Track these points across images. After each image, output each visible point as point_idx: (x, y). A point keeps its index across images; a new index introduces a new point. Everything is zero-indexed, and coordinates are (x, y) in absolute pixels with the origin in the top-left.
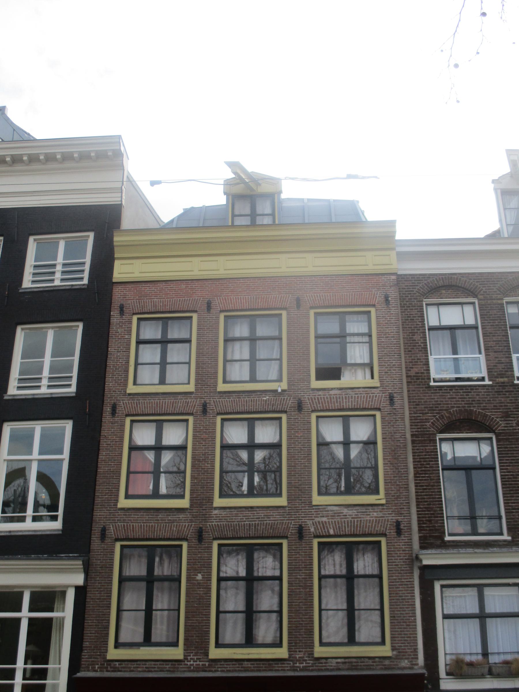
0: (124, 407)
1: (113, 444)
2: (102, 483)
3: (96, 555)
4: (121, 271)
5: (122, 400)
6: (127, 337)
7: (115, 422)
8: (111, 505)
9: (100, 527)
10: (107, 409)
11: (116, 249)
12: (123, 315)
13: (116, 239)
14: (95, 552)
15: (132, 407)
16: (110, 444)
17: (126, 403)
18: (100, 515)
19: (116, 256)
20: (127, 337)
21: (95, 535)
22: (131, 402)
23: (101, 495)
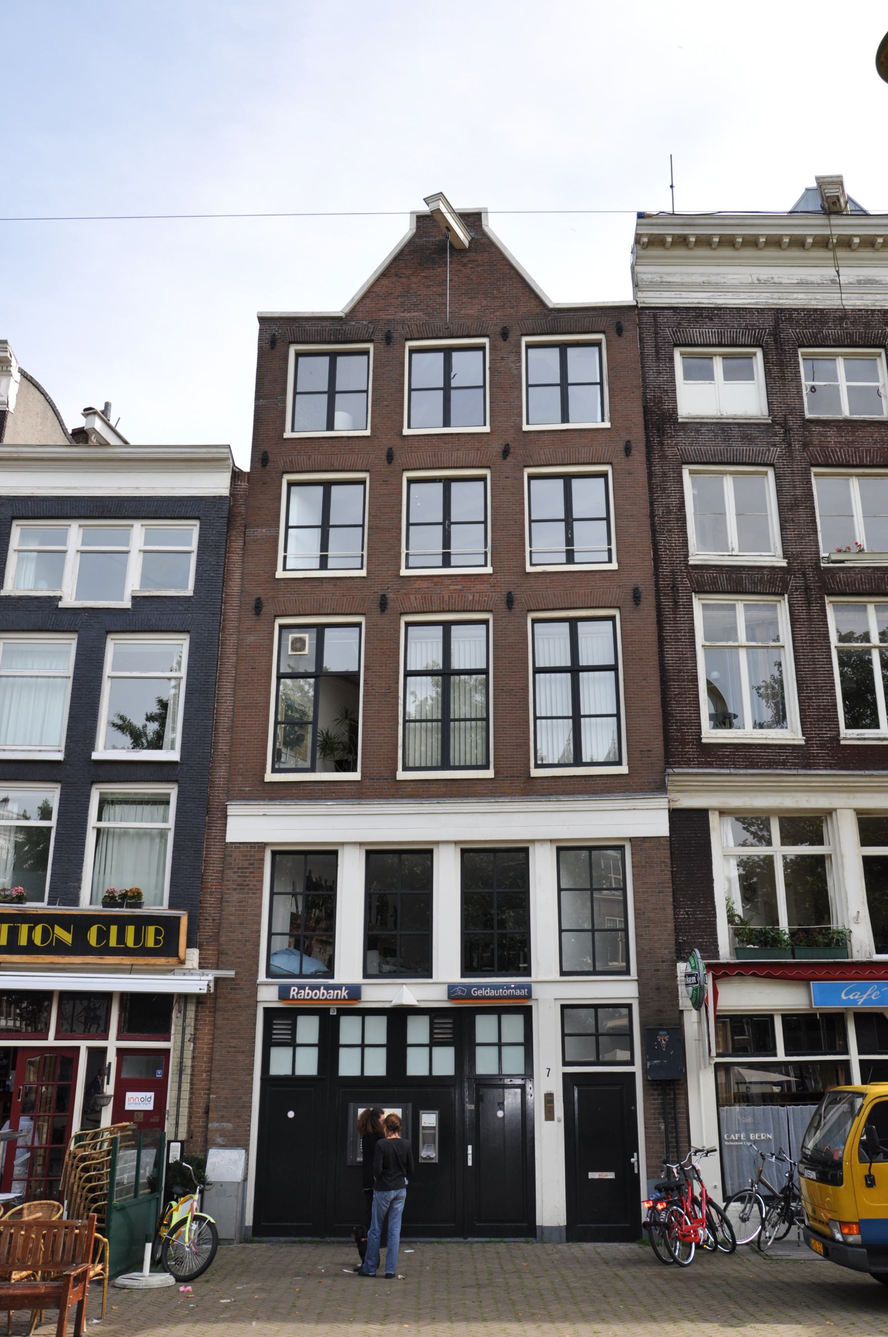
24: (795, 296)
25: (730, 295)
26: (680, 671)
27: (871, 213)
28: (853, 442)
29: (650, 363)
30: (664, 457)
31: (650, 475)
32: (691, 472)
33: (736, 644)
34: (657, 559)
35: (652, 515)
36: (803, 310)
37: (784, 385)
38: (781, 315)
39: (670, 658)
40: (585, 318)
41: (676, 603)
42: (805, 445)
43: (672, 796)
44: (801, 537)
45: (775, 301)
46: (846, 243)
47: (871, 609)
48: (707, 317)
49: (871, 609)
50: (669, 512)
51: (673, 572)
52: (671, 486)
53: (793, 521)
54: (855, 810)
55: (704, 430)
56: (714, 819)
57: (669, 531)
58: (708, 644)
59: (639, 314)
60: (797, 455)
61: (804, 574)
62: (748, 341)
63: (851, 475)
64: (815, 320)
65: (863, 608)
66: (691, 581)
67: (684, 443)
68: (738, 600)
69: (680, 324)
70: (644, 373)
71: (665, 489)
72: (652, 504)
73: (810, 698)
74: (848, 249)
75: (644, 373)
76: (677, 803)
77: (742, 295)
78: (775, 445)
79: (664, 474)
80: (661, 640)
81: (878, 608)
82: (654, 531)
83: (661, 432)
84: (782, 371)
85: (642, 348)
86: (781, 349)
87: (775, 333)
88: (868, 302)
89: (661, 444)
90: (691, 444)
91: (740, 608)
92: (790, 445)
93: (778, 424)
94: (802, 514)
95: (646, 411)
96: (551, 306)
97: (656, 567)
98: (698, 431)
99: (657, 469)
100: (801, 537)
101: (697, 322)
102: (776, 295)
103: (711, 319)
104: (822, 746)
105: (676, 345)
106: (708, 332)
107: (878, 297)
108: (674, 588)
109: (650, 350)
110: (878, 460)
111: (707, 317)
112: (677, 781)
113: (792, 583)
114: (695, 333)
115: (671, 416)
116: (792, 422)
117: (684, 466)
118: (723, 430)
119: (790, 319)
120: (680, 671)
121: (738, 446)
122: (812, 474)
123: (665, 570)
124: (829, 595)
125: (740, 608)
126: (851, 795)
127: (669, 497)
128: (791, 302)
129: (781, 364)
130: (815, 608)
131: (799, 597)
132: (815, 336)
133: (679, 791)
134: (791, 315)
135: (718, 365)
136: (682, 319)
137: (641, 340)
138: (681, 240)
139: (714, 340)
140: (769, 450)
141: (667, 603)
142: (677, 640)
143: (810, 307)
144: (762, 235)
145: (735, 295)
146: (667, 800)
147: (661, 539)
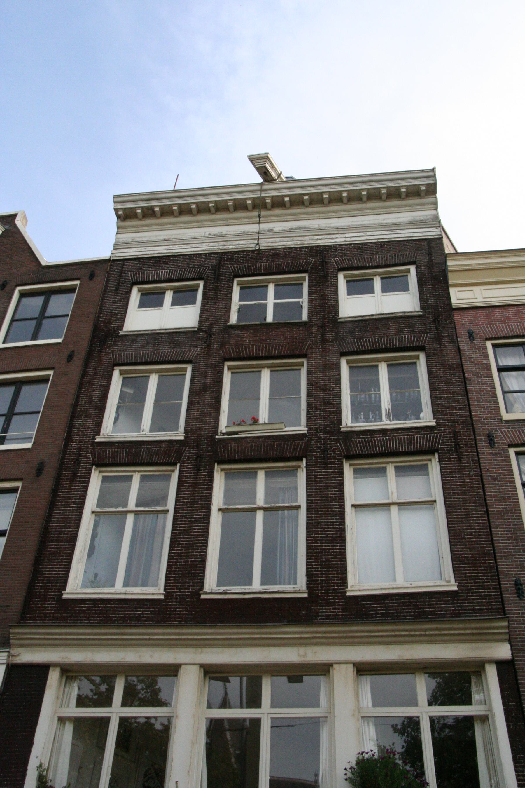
0: (504, 436)
1: (501, 478)
2: (499, 525)
3: (517, 617)
4: (458, 297)
5: (499, 429)
6: (485, 362)
7: (497, 454)
8: (519, 552)
9: (512, 581)
10: (482, 440)
11: (450, 276)
12: (474, 340)
13: (449, 263)
14: (514, 614)
15: (515, 436)
16: (497, 479)
17: (505, 431)
18: (507, 565)
19: (451, 282)
20: (485, 362)
21: (508, 591)
22: (512, 431)
23: (502, 540)
24: (237, 242)
25: (185, 246)
26: (60, 533)
27: (297, 178)
28: (266, 339)
29: (110, 296)
30: (100, 361)
31: (84, 375)
32: (122, 373)
33: (124, 509)
34: (68, 439)
35: (75, 405)
36: (243, 252)
37: (215, 303)
38: (224, 257)
39: (55, 521)
40: (67, 271)
41: (75, 475)
42: (222, 345)
43: (14, 651)
44: (202, 415)
45: (220, 248)
46: (278, 203)
47: (261, 476)
48: (163, 263)
49: (261, 476)
50: (91, 401)
51: (80, 449)
52: (99, 383)
53: (198, 403)
54: (201, 666)
55: (138, 339)
56: (54, 677)
57: (87, 416)
58: (98, 510)
59: (111, 265)
60: (214, 353)
61: (198, 446)
62: (192, 275)
63: (263, 367)
64: (251, 258)
65: (253, 474)
66: (94, 455)
67: (120, 351)
68: (135, 471)
69: (141, 269)
70: (102, 304)
71: (93, 384)
72: (78, 396)
73: (179, 555)
74: (284, 208)
75: (102, 304)
76: (17, 658)
77: (194, 246)
78: (196, 347)
79: (96, 374)
80: (52, 505)
81: (269, 474)
82: (73, 417)
83: (103, 342)
84: (216, 294)
85: (107, 286)
86: (218, 279)
87: (216, 269)
88: (298, 243)
89: (100, 352)
90: (125, 351)
91: (136, 479)
92: (209, 345)
93: (203, 331)
94: (208, 397)
95: (96, 329)
96: (43, 264)
97: (66, 445)
98: (133, 341)
99: (91, 371)
100: (202, 415)
101: (155, 266)
102: (222, 243)
103: (167, 264)
104: (181, 601)
105: (134, 283)
106: (162, 272)
107: (307, 238)
108: (78, 462)
109: (112, 287)
110: (286, 352)
111: (163, 263)
112: (19, 634)
113: (187, 453)
114: (151, 274)
115: (115, 331)
116: (215, 329)
117: (115, 368)
118: (155, 339)
119: (231, 259)
120: (60, 533)
121: (165, 350)
122: (226, 368)
123: (74, 447)
124: (220, 462)
125: (136, 479)
126: (199, 650)
127: (94, 391)
128: (234, 247)
129: (216, 289)
130: (203, 473)
131: (189, 465)
132: (249, 268)
133: (22, 646)
134: (233, 256)
135: (169, 296)
136: (143, 265)
137: (107, 282)
138: (150, 212)
139: (165, 277)
140: (190, 351)
141: (67, 474)
142: (67, 505)
143: (249, 249)
144: (211, 201)
145: (189, 246)
146: (6, 654)
147: (78, 424)
